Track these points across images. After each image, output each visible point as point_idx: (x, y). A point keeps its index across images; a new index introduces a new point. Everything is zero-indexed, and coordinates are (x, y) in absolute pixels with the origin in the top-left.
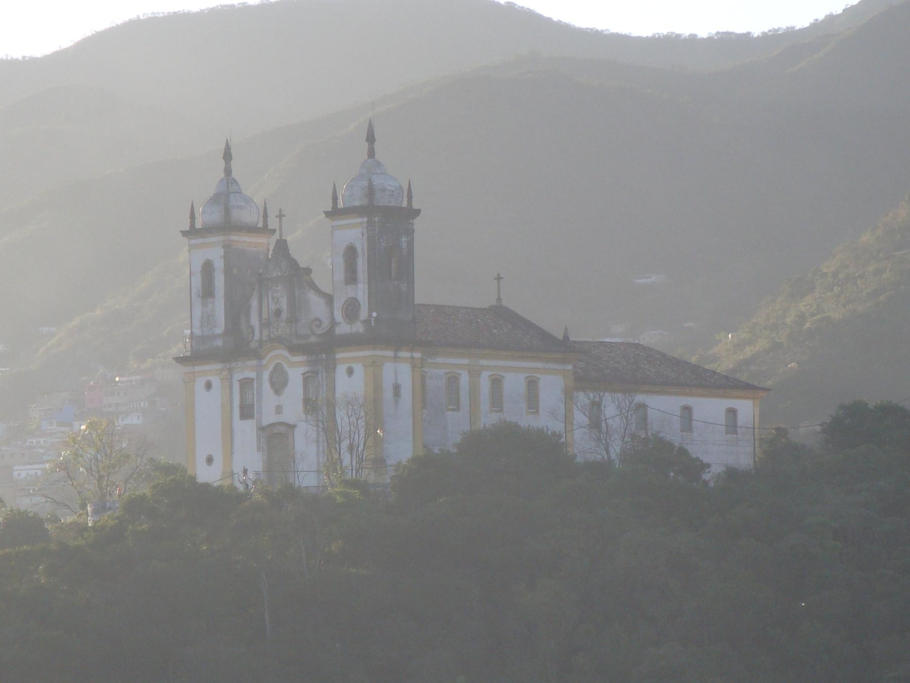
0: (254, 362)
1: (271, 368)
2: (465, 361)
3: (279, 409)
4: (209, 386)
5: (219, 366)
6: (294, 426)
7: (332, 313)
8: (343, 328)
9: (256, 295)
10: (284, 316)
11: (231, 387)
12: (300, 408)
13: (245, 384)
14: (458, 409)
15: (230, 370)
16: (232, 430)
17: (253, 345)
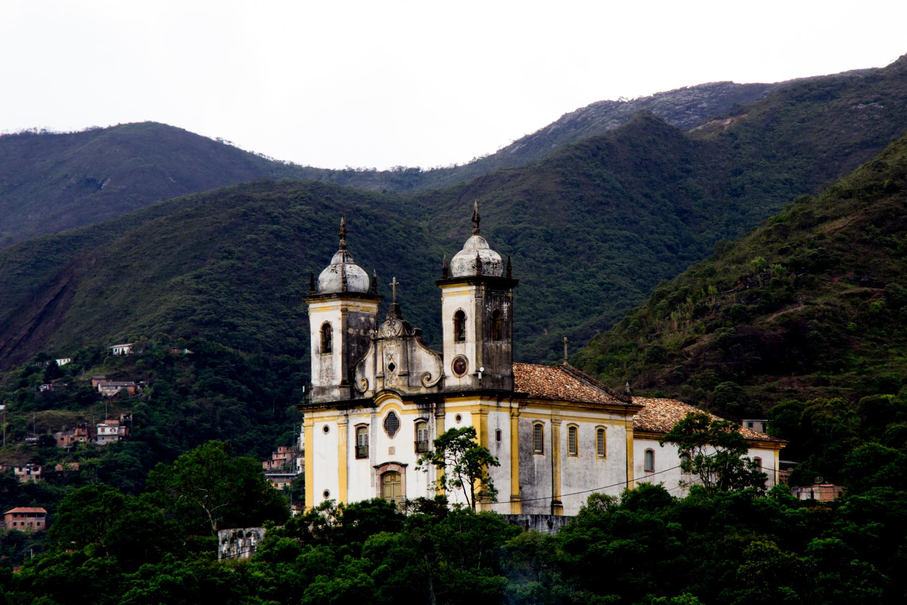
0: (370, 410)
1: (385, 415)
2: (549, 412)
3: (392, 451)
4: (326, 429)
5: (337, 413)
6: (405, 466)
7: (441, 368)
8: (453, 381)
9: (371, 351)
10: (398, 370)
11: (347, 432)
12: (412, 447)
13: (360, 428)
14: (542, 453)
15: (347, 415)
16: (347, 468)
17: (368, 395)
